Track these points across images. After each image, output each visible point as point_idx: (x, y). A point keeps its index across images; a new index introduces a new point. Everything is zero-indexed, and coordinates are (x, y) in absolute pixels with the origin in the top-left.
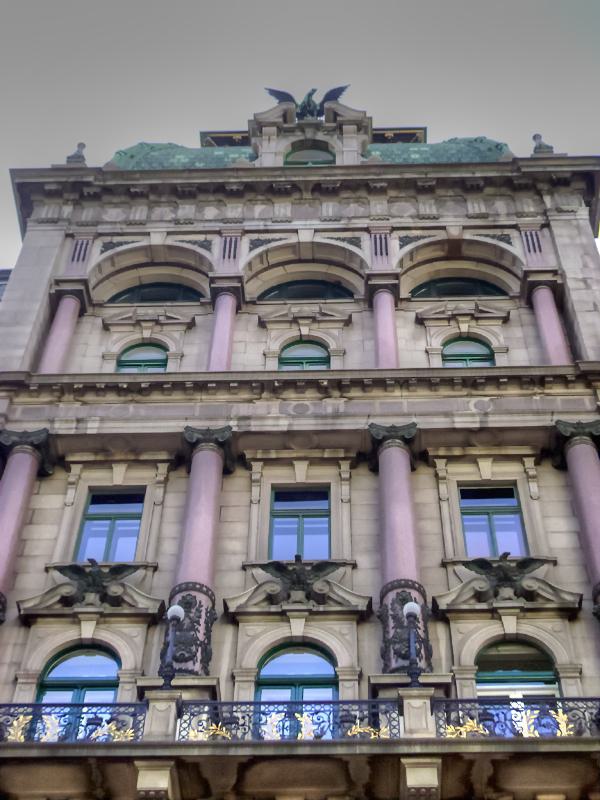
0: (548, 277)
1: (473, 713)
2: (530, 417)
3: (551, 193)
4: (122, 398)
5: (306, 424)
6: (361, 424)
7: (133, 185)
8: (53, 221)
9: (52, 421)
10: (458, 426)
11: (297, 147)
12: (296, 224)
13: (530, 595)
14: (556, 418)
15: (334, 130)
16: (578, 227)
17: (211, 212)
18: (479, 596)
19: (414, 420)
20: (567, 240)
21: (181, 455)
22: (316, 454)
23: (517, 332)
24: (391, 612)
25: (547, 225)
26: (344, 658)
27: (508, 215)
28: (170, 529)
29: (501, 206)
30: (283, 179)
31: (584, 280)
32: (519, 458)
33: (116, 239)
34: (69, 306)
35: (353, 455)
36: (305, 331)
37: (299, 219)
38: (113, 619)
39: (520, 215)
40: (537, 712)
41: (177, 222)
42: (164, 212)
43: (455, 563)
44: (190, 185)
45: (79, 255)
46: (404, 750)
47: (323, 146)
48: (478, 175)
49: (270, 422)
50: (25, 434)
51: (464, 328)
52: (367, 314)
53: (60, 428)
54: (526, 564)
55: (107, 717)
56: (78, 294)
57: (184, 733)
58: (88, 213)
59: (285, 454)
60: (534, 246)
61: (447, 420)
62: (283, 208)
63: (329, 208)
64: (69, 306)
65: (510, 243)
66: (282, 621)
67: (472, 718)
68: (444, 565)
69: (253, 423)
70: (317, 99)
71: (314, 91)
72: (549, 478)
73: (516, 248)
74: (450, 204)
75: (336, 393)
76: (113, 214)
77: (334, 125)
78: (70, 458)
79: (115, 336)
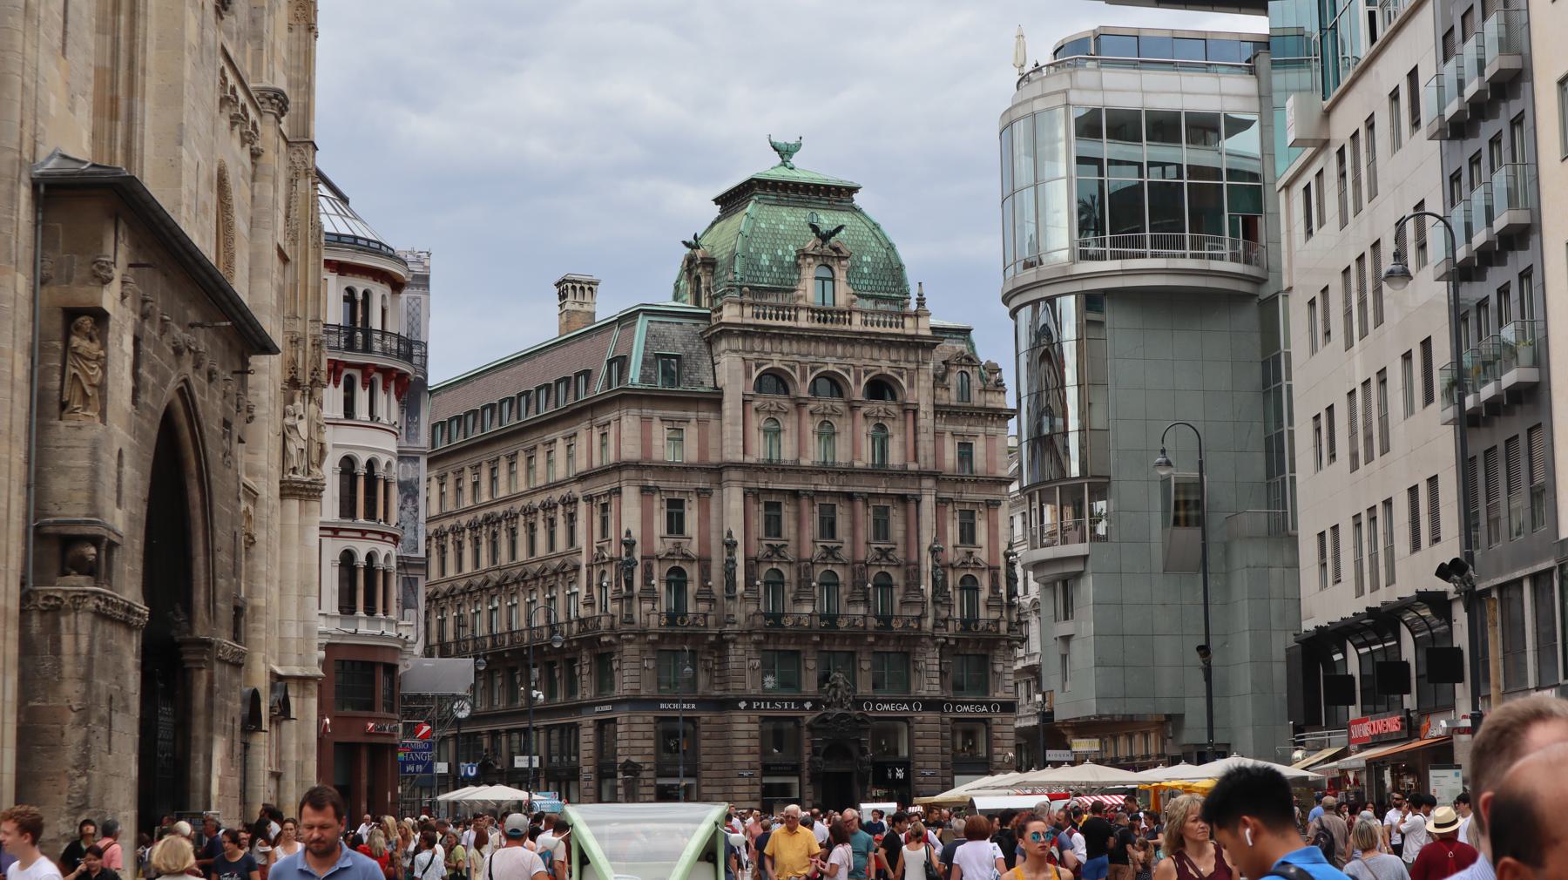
5: (834, 489)
17: (795, 346)
23: (897, 424)
26: (841, 579)
42: (776, 343)
47: (830, 268)
53: (762, 486)
58: (748, 343)
60: (911, 385)
62: (822, 348)
63: (839, 349)
72: (900, 506)
73: (904, 383)
76: (757, 344)
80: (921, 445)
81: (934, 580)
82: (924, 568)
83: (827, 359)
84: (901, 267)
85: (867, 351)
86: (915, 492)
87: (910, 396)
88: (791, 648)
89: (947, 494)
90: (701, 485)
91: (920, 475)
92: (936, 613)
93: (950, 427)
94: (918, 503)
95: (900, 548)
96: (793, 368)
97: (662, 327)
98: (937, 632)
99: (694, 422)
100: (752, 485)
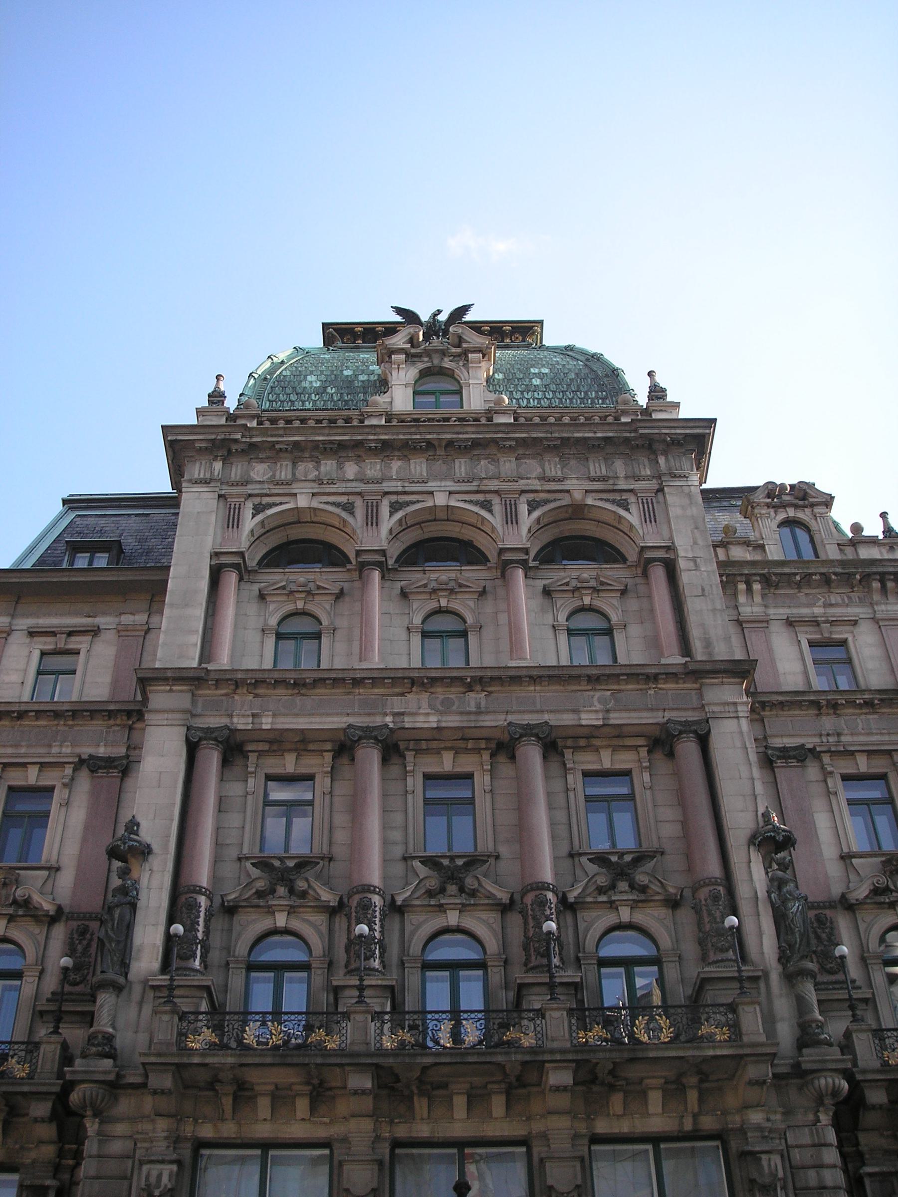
0: (661, 554)
1: (597, 1019)
2: (645, 714)
3: (665, 453)
4: (290, 692)
5: (452, 721)
6: (500, 720)
7: (278, 442)
8: (205, 482)
9: (231, 716)
10: (584, 723)
11: (424, 374)
12: (432, 485)
13: (644, 889)
14: (668, 715)
15: (459, 355)
16: (689, 495)
17: (351, 469)
18: (601, 890)
19: (546, 717)
20: (679, 511)
21: (344, 747)
22: (461, 744)
23: (633, 604)
24: (530, 912)
25: (661, 490)
27: (626, 477)
28: (341, 819)
29: (620, 467)
30: (418, 437)
31: (694, 559)
32: (636, 748)
33: (266, 500)
34: (231, 578)
35: (493, 745)
36: (444, 603)
37: (435, 478)
38: (301, 910)
39: (637, 478)
40: (646, 1018)
41: (319, 481)
42: (306, 468)
43: (581, 855)
44: (331, 442)
45: (232, 520)
46: (547, 1057)
48: (599, 435)
49: (421, 718)
50: (209, 730)
51: (587, 600)
52: (499, 582)
53: (241, 723)
54: (640, 858)
55: (317, 1024)
56: (236, 566)
57: (378, 1045)
58: (236, 471)
59: (434, 744)
60: (649, 516)
61: (575, 717)
62: (419, 466)
63: (461, 466)
64: (231, 578)
65: (628, 510)
66: (440, 911)
67: (598, 1024)
68: (571, 855)
69: (406, 719)
70: (443, 317)
71: (439, 312)
73: (633, 517)
74: (573, 462)
75: (478, 688)
76: (259, 471)
77: (459, 350)
78: (250, 747)
79: (272, 607)
80: (693, 620)
81: (780, 918)
82: (743, 891)
83: (432, 485)
84: (614, 374)
85: (532, 467)
86: (692, 716)
87: (650, 537)
88: (297, 1131)
89: (791, 732)
90: (102, 751)
91: (698, 674)
92: (801, 1004)
93: (779, 612)
94: (704, 741)
95: (673, 861)
96: (349, 508)
97: (102, 521)
98: (810, 1056)
99: (109, 636)
100: (214, 721)
